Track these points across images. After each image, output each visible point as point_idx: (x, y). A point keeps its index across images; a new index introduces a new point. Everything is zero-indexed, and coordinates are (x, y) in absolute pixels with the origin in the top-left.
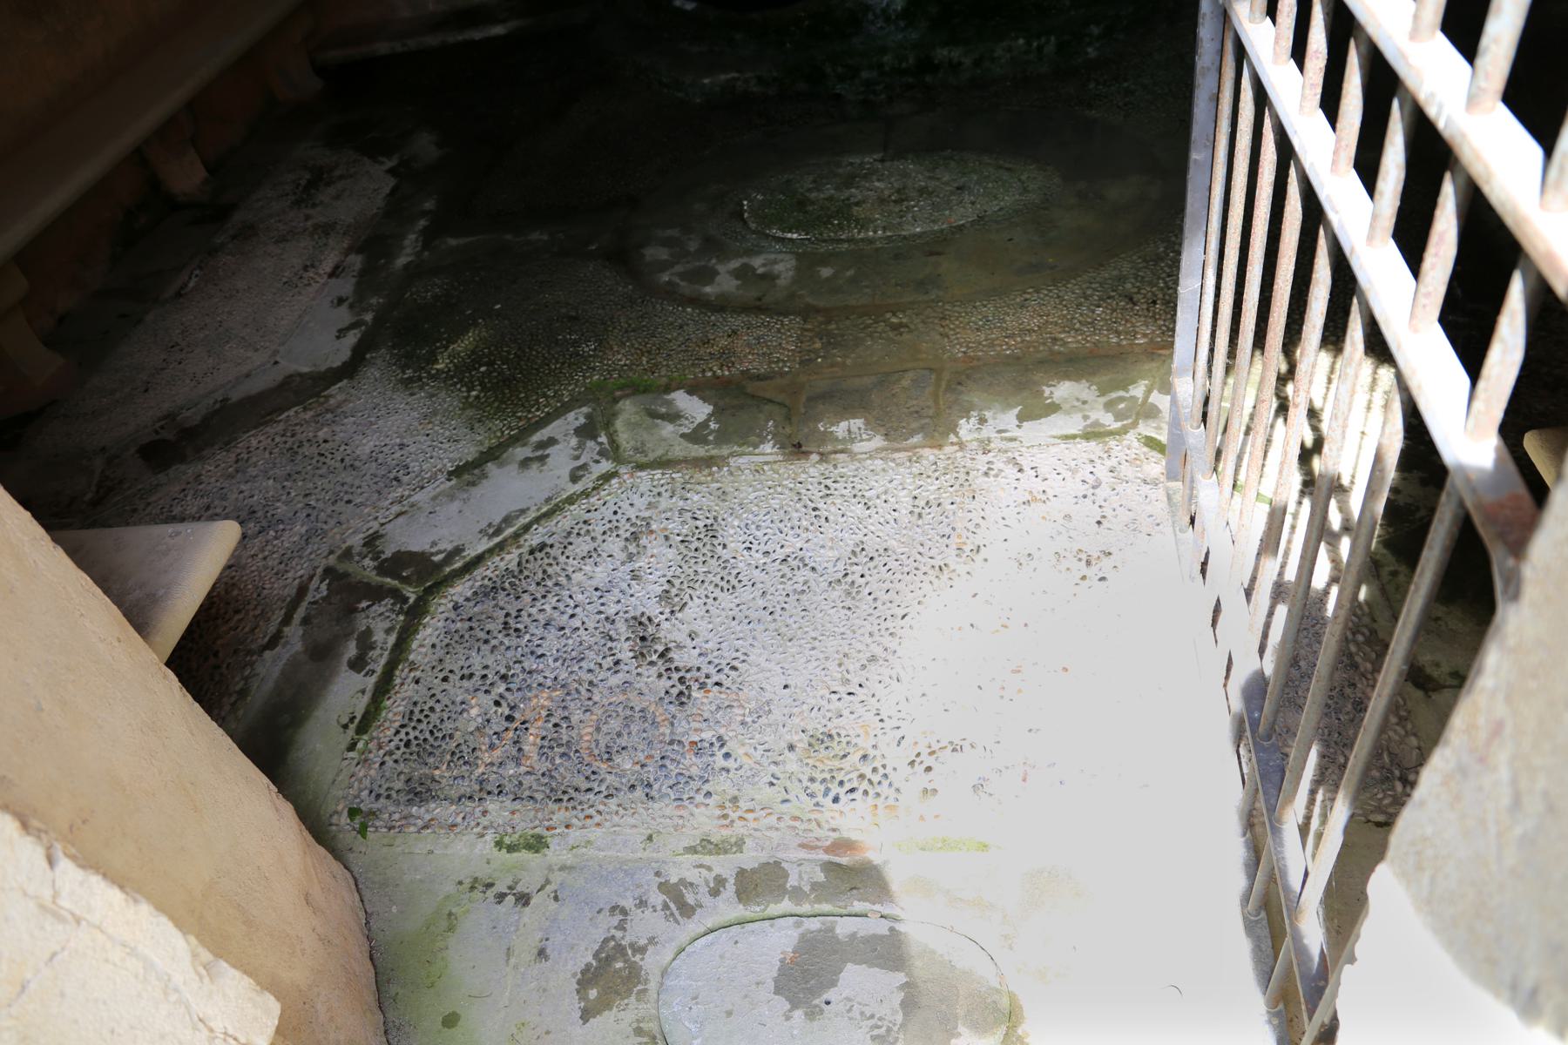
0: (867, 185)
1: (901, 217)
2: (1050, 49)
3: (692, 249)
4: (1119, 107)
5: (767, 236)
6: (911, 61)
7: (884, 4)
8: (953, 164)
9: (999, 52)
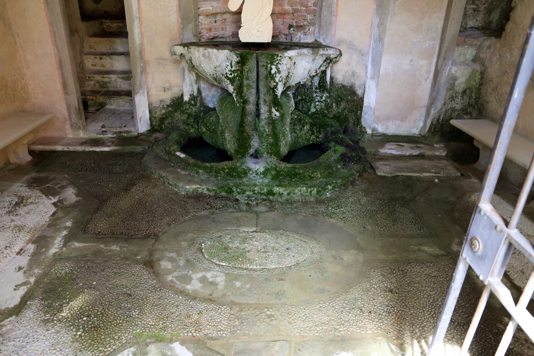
0: (252, 243)
1: (266, 260)
2: (314, 192)
4: (341, 219)
5: (213, 263)
7: (256, 169)
9: (296, 191)
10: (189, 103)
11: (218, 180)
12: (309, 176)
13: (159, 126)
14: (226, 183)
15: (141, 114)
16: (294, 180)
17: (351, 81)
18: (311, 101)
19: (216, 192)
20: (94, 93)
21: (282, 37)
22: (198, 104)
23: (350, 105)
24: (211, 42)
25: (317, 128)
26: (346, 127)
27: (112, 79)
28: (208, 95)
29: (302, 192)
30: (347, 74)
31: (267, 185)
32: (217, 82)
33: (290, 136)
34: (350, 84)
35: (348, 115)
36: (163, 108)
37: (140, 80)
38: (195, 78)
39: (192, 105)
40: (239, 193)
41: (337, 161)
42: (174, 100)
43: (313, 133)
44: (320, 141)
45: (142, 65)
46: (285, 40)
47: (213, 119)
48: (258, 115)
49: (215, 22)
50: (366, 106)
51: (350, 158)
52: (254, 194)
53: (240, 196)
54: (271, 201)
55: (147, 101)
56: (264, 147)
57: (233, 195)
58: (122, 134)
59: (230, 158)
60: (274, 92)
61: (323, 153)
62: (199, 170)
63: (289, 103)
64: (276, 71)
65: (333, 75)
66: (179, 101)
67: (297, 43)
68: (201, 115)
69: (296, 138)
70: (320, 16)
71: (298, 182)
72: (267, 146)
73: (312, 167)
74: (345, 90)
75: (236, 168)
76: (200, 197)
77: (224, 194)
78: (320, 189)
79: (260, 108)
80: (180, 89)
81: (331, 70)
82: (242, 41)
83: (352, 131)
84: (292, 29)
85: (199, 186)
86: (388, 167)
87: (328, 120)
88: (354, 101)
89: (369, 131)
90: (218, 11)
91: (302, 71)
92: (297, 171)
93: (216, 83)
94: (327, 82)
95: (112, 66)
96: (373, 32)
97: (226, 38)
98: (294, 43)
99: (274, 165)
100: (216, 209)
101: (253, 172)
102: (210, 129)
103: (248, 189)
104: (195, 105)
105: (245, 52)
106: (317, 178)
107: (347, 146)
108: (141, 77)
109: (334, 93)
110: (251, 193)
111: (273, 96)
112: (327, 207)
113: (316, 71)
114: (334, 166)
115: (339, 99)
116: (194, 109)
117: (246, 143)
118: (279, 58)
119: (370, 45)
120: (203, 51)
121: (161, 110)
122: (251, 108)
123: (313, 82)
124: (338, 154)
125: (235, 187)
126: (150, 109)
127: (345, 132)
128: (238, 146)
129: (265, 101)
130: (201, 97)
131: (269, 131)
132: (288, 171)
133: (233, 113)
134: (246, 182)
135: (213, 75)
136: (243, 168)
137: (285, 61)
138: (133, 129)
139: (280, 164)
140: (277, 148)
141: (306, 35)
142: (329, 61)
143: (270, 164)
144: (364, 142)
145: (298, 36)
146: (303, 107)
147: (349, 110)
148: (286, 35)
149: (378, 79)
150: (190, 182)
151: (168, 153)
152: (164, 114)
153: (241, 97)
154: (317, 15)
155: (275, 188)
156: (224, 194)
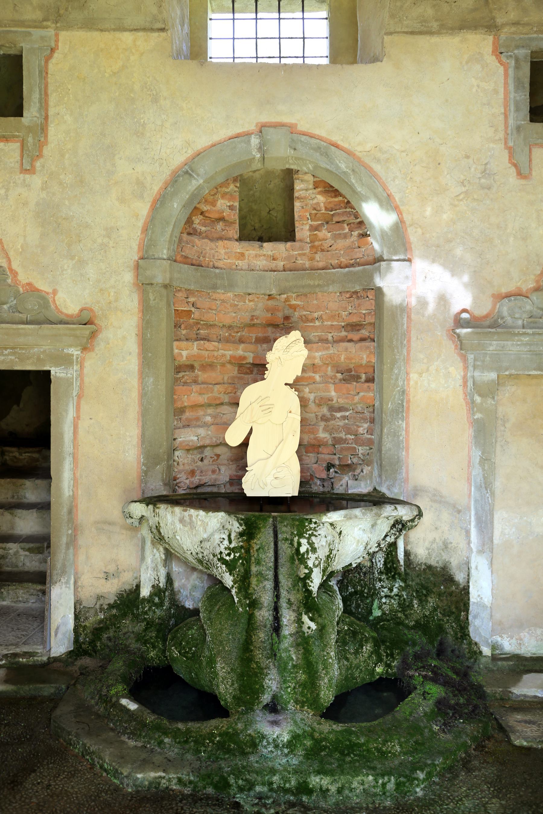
2: (391, 786)
6: (293, 783)
7: (275, 736)
9: (355, 785)
10: (149, 600)
11: (199, 759)
13: (90, 643)
14: (215, 766)
15: (60, 621)
16: (348, 759)
17: (443, 558)
18: (372, 596)
19: (195, 787)
21: (316, 484)
22: (167, 604)
23: (445, 602)
24: (194, 494)
25: (387, 648)
26: (441, 644)
28: (184, 586)
29: (366, 786)
30: (434, 545)
31: (296, 772)
32: (202, 566)
33: (336, 666)
34: (440, 563)
35: (443, 621)
36: (101, 609)
38: (164, 557)
39: (156, 605)
40: (241, 789)
41: (431, 716)
42: (122, 594)
43: (380, 660)
44: (395, 673)
45: (70, 532)
46: (321, 488)
47: (193, 632)
48: (277, 628)
49: (202, 460)
50: (474, 603)
51: (455, 709)
54: (304, 806)
55: (73, 597)
56: (289, 690)
57: (229, 794)
58: (17, 660)
59: (224, 713)
60: (305, 585)
61: (403, 699)
62: (163, 737)
63: (333, 602)
64: (308, 549)
65: (409, 548)
66: (130, 597)
67: (342, 494)
69: (348, 669)
70: (380, 450)
71: (357, 764)
72: (294, 688)
74: (433, 574)
75: (236, 734)
76: (163, 798)
77: (210, 790)
79: (281, 615)
80: (135, 575)
81: (404, 540)
82: (248, 495)
83: (453, 651)
84: (332, 470)
85: (163, 774)
87: (406, 632)
88: (451, 594)
89: (486, 651)
90: (207, 442)
91: (354, 546)
93: (201, 567)
94: (398, 561)
95: (12, 528)
96: (473, 473)
97: (218, 486)
98: (337, 494)
99: (309, 726)
101: (269, 743)
102: (188, 652)
103: (259, 779)
104: (161, 605)
105: (254, 516)
106: (394, 754)
107: (447, 683)
108: (66, 553)
109: (413, 581)
111: (305, 592)
114: (425, 727)
115: (424, 592)
117: (256, 683)
118: (313, 526)
119: (470, 495)
120: (180, 513)
121: (96, 614)
123: (374, 561)
124: (431, 702)
125: (234, 774)
126: (78, 611)
127: (440, 653)
128: (240, 689)
129: (289, 602)
130: (172, 590)
131: (298, 658)
132: (337, 739)
134: (256, 765)
135: (197, 553)
136: (250, 735)
137: (322, 531)
138: (39, 649)
139: (320, 724)
140: (313, 692)
141: (356, 480)
142: (400, 526)
143: (302, 725)
144: (479, 674)
145: (344, 482)
146: (358, 606)
147: (444, 610)
148: (323, 480)
149: (492, 552)
152: (101, 621)
153: (247, 596)
154: (375, 447)
155: (313, 778)
156: (210, 790)
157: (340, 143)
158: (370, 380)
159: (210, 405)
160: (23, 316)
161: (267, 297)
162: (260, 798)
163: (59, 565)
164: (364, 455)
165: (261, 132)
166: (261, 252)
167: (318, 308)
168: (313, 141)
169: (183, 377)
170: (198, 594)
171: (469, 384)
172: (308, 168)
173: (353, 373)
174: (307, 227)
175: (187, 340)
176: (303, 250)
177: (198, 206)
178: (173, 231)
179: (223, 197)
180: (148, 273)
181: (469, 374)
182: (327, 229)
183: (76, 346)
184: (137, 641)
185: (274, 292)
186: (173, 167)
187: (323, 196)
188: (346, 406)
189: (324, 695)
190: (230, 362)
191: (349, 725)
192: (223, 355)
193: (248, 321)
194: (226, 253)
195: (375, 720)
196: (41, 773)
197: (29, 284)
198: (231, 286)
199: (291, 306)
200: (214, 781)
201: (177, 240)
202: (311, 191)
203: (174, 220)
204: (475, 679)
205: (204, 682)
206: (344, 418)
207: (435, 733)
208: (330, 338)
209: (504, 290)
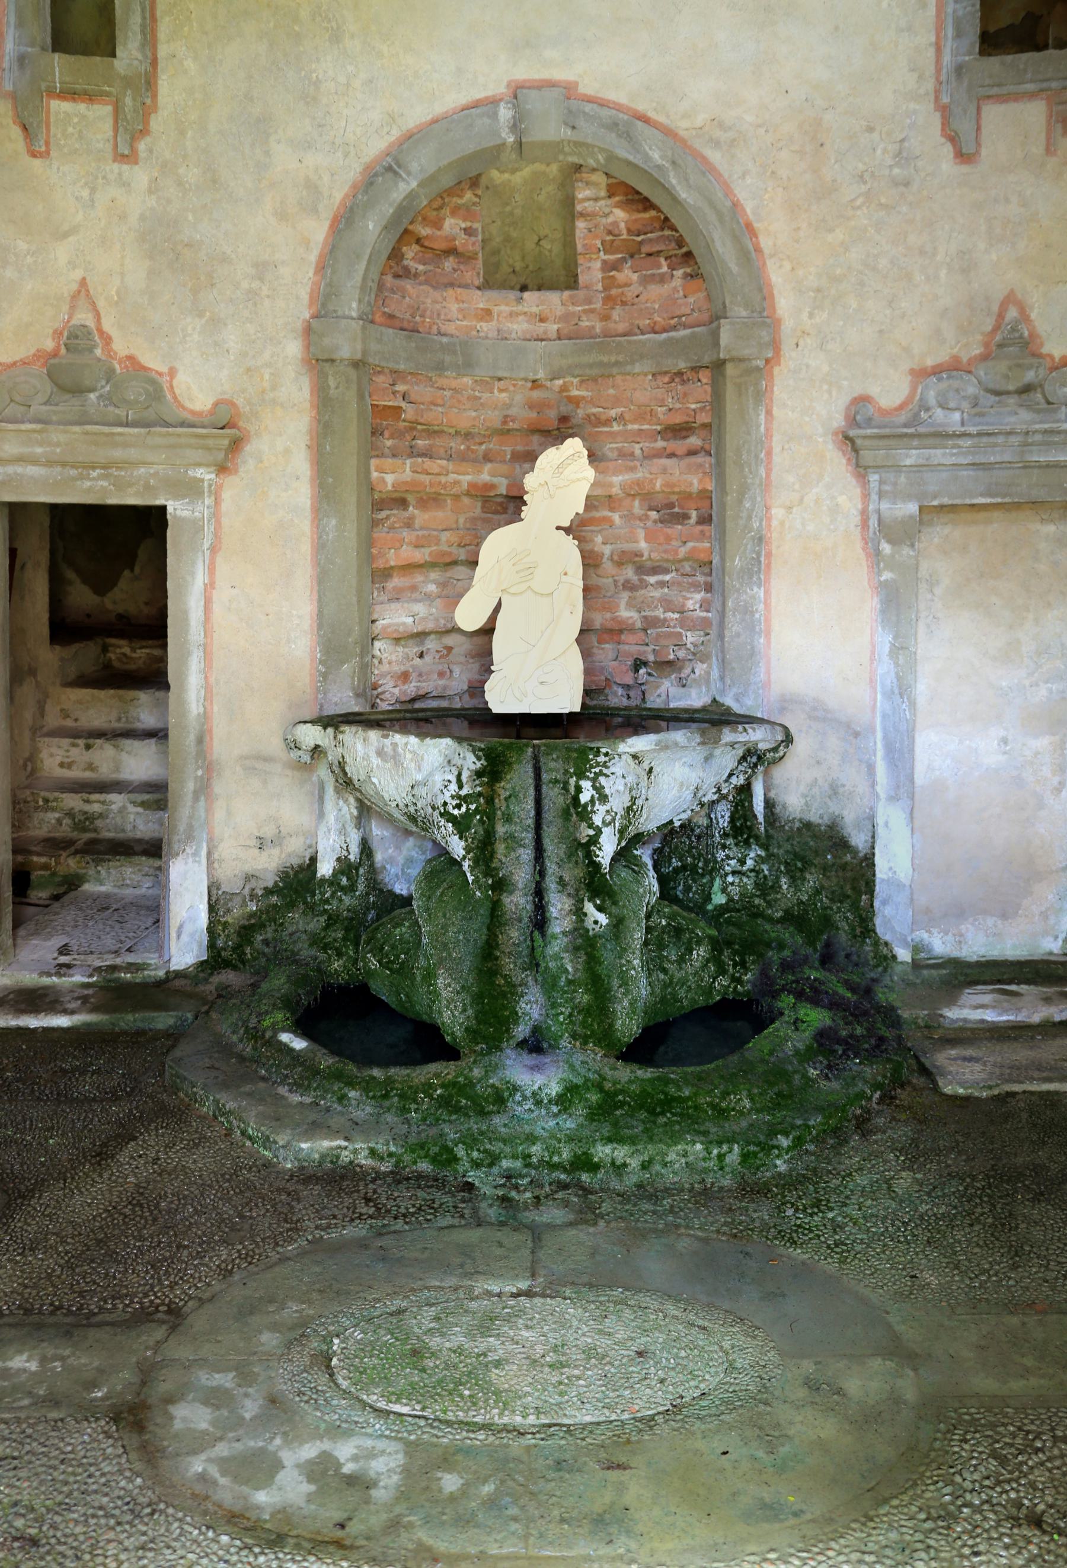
0: (512, 1333)
3: (247, 1416)
4: (829, 1247)
5: (364, 1404)
6: (564, 1156)
8: (628, 1313)
10: (333, 882)
11: (407, 1121)
12: (714, 1106)
13: (234, 949)
14: (433, 1131)
16: (662, 1120)
19: (398, 1162)
20: (55, 845)
22: (361, 887)
24: (406, 711)
27: (113, 807)
31: (570, 1139)
36: (253, 896)
37: (191, 817)
38: (355, 813)
39: (342, 888)
40: (476, 1165)
42: (286, 873)
52: (528, 1165)
53: (479, 1173)
57: (456, 1171)
58: (116, 975)
59: (451, 1053)
67: (658, 710)
68: (370, 917)
70: (721, 636)
71: (677, 1127)
73: (722, 1077)
75: (471, 1084)
76: (343, 1177)
77: (424, 1166)
78: (752, 1148)
80: (308, 842)
85: (344, 1143)
86: (978, 1067)
92: (672, 1090)
97: (450, 698)
99: (596, 1072)
100: (396, 1218)
101: (525, 1098)
102: (393, 962)
103: (508, 1149)
104: (352, 888)
108: (193, 807)
110: (518, 1164)
112: (778, 1207)
113: (719, 790)
116: (347, 900)
119: (874, 706)
121: (244, 904)
122: (518, 902)
125: (464, 1143)
130: (372, 865)
132: (644, 1091)
133: (464, 918)
134: (503, 1129)
136: (493, 1086)
138: (152, 959)
139: (616, 1069)
142: (754, 759)
143: (583, 1071)
149: (913, 799)
150: (314, 1129)
151: (255, 1035)
152: (252, 915)
154: (714, 632)
155: (599, 1148)
157: (651, 114)
158: (705, 520)
159: (432, 565)
160: (121, 412)
161: (529, 385)
162: (509, 1177)
163: (182, 827)
164: (695, 646)
165: (515, 97)
166: (520, 308)
167: (617, 402)
168: (605, 113)
169: (388, 518)
170: (415, 871)
171: (871, 523)
172: (597, 161)
173: (676, 510)
174: (598, 264)
175: (394, 456)
176: (590, 303)
177: (411, 227)
178: (367, 270)
179: (454, 212)
180: (326, 341)
181: (871, 507)
182: (631, 267)
183: (208, 465)
184: (311, 945)
185: (541, 375)
186: (367, 159)
187: (623, 210)
188: (665, 565)
189: (623, 1024)
190: (468, 494)
191: (666, 1070)
192: (456, 483)
193: (497, 424)
194: (460, 310)
195: (710, 1062)
196: (144, 1141)
197: (130, 358)
198: (468, 365)
199: (571, 400)
200: (431, 1153)
201: (374, 286)
202: (602, 203)
203: (368, 251)
204: (882, 996)
205: (420, 1007)
206: (662, 584)
207: (812, 1080)
208: (638, 452)
209: (930, 362)
